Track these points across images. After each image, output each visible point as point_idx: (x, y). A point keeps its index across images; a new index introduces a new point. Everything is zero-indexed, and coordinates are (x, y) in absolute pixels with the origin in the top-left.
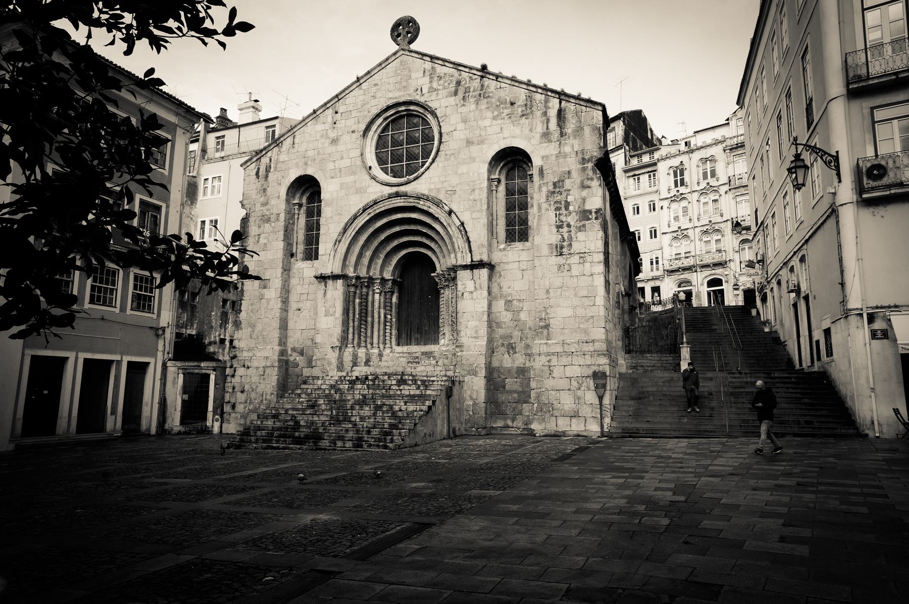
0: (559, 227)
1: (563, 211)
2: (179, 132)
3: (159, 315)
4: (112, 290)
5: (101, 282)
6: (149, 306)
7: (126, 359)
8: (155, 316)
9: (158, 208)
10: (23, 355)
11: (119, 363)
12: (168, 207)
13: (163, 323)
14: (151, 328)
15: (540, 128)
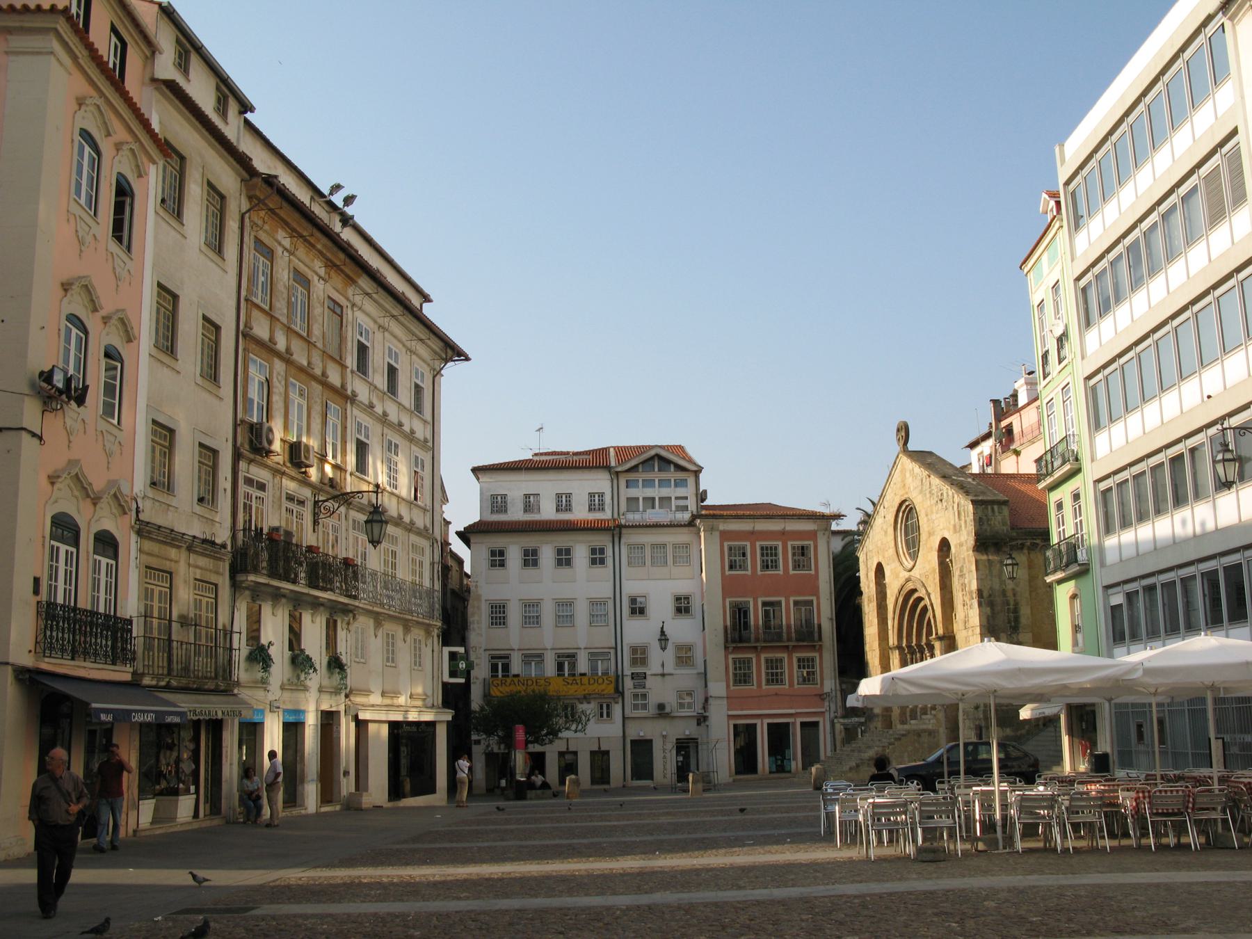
0: (964, 605)
1: (964, 593)
2: (820, 535)
3: (822, 684)
4: (781, 673)
5: (772, 669)
6: (814, 679)
7: (799, 720)
8: (819, 686)
9: (810, 603)
10: (728, 724)
11: (794, 723)
12: (818, 599)
13: (827, 689)
14: (816, 695)
15: (952, 522)
